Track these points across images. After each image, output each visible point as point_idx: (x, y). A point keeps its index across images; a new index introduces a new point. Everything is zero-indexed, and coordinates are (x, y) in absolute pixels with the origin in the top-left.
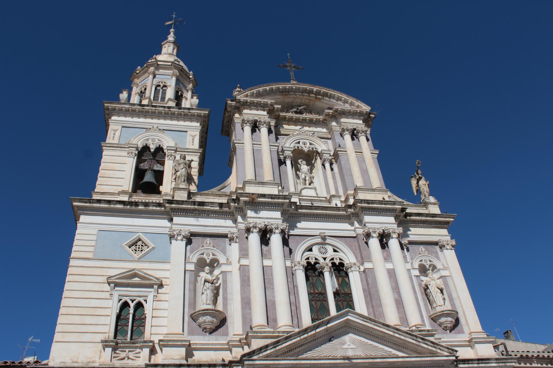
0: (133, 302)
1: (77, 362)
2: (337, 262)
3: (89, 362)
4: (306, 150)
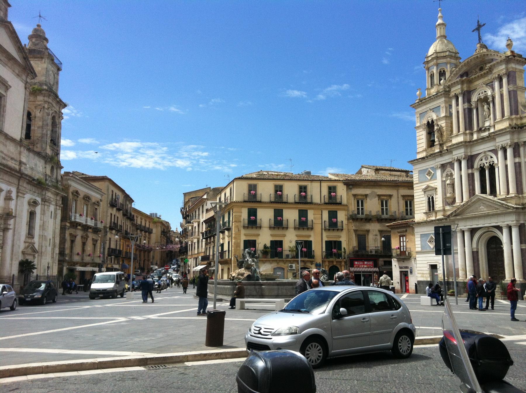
2: (491, 163)
4: (482, 97)
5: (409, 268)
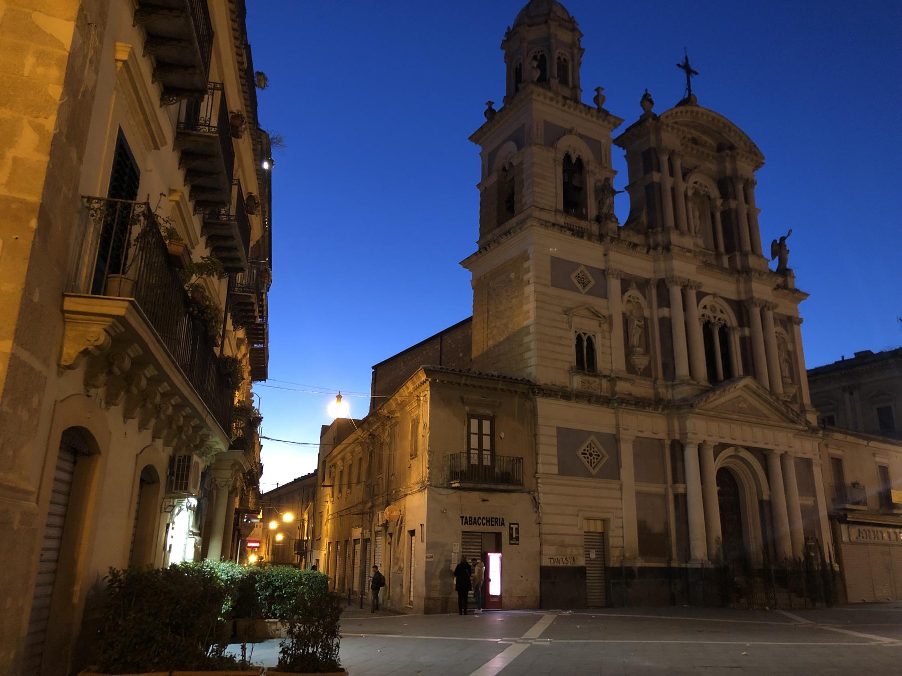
0: (585, 335)
1: (555, 386)
3: (563, 387)
5: (507, 524)
